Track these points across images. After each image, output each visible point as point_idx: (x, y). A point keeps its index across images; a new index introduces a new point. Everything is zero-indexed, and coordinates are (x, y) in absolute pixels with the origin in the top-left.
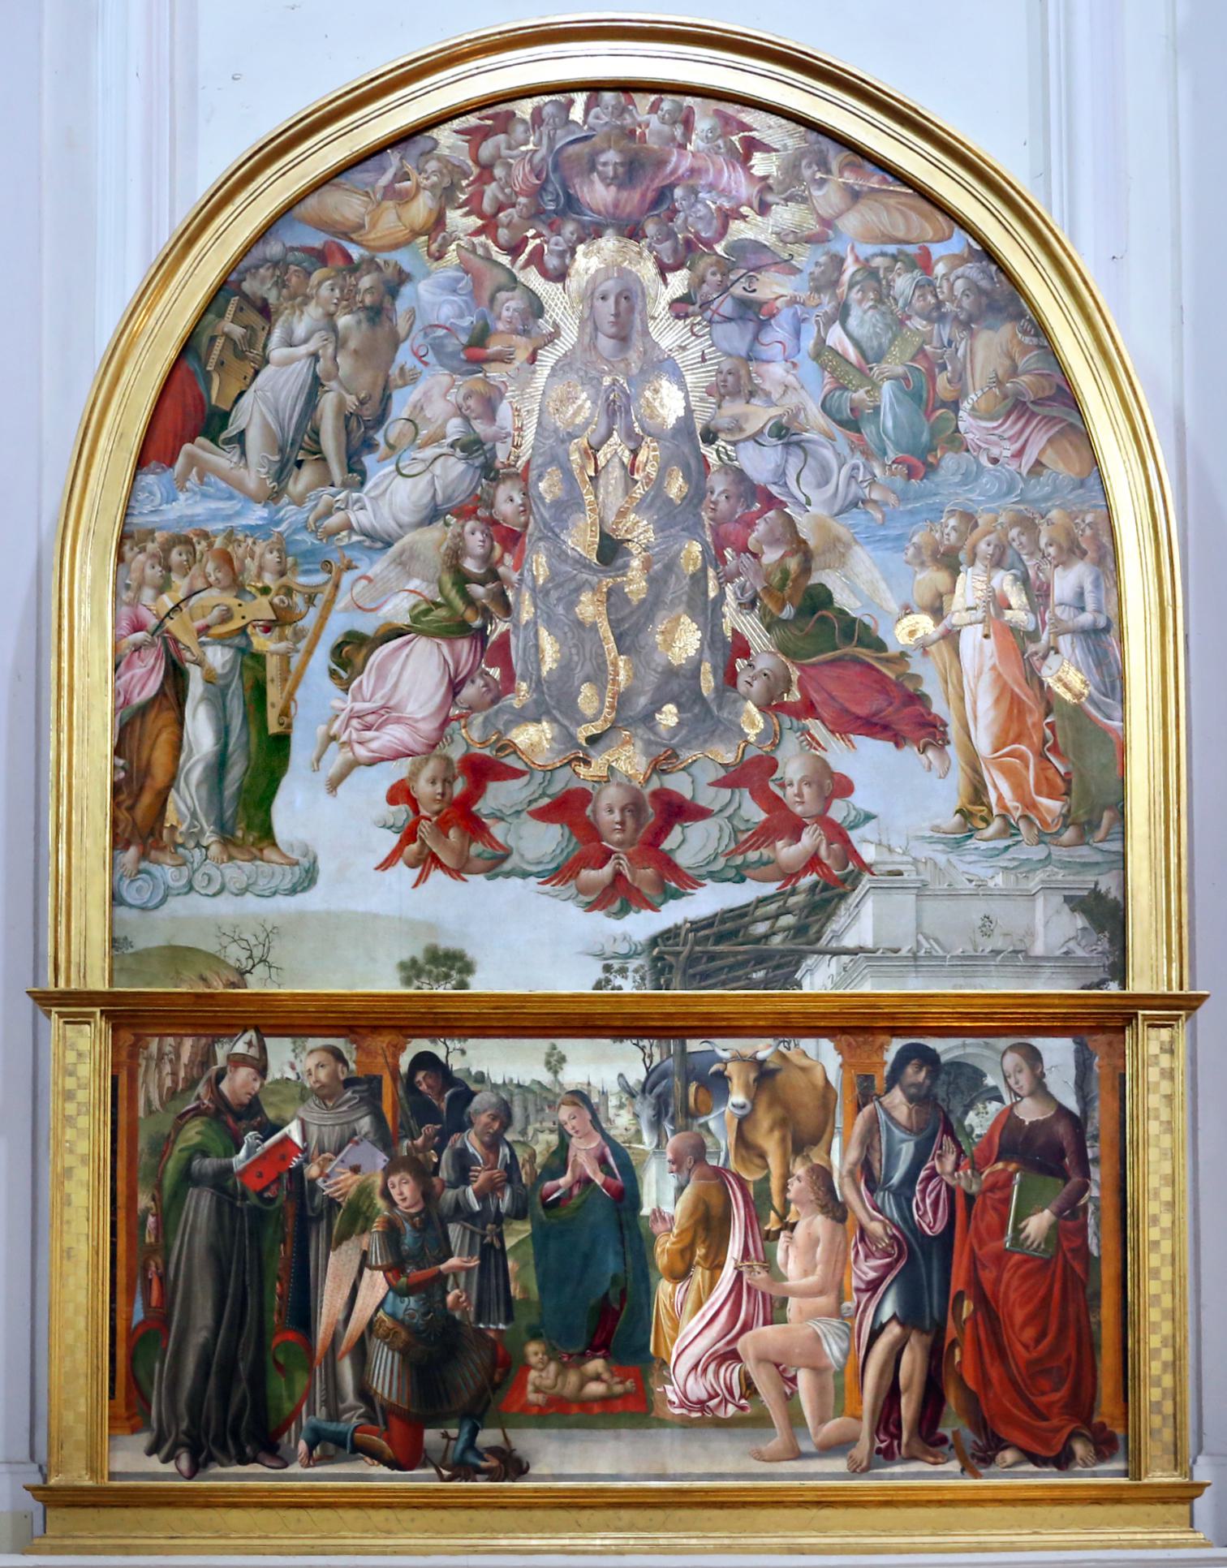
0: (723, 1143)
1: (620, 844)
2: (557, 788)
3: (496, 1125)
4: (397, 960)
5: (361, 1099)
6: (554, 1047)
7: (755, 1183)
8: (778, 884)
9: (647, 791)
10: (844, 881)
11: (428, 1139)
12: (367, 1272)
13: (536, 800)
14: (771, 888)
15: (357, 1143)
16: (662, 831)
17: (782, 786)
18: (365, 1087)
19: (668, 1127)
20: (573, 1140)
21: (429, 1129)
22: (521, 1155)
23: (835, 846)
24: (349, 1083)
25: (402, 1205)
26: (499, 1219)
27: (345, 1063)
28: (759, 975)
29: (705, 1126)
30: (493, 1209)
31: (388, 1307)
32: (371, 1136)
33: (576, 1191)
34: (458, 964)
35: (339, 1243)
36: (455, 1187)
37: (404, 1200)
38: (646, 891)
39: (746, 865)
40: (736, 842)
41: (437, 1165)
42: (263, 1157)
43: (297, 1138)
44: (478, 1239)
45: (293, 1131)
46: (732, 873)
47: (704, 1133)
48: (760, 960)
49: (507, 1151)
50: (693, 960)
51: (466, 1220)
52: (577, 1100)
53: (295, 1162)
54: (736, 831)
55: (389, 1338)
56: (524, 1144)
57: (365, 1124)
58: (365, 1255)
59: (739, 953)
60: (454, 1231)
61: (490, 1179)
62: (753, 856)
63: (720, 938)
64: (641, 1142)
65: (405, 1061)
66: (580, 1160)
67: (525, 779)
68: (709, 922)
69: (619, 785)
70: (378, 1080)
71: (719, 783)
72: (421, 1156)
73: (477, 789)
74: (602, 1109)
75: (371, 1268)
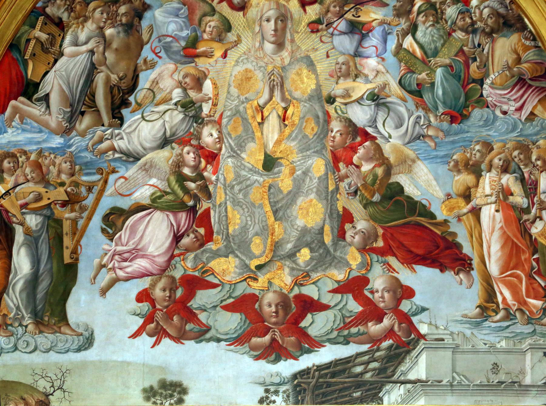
1: (275, 324)
2: (238, 292)
4: (142, 388)
8: (369, 345)
9: (291, 295)
10: (409, 343)
13: (225, 300)
14: (365, 348)
16: (302, 317)
17: (372, 292)
23: (403, 325)
28: (357, 395)
34: (178, 389)
38: (290, 349)
39: (350, 335)
40: (344, 322)
46: (342, 339)
48: (358, 385)
50: (317, 387)
54: (344, 317)
59: (346, 382)
62: (354, 330)
63: (334, 375)
67: (220, 288)
68: (328, 366)
69: (275, 292)
71: (334, 291)
73: (190, 295)
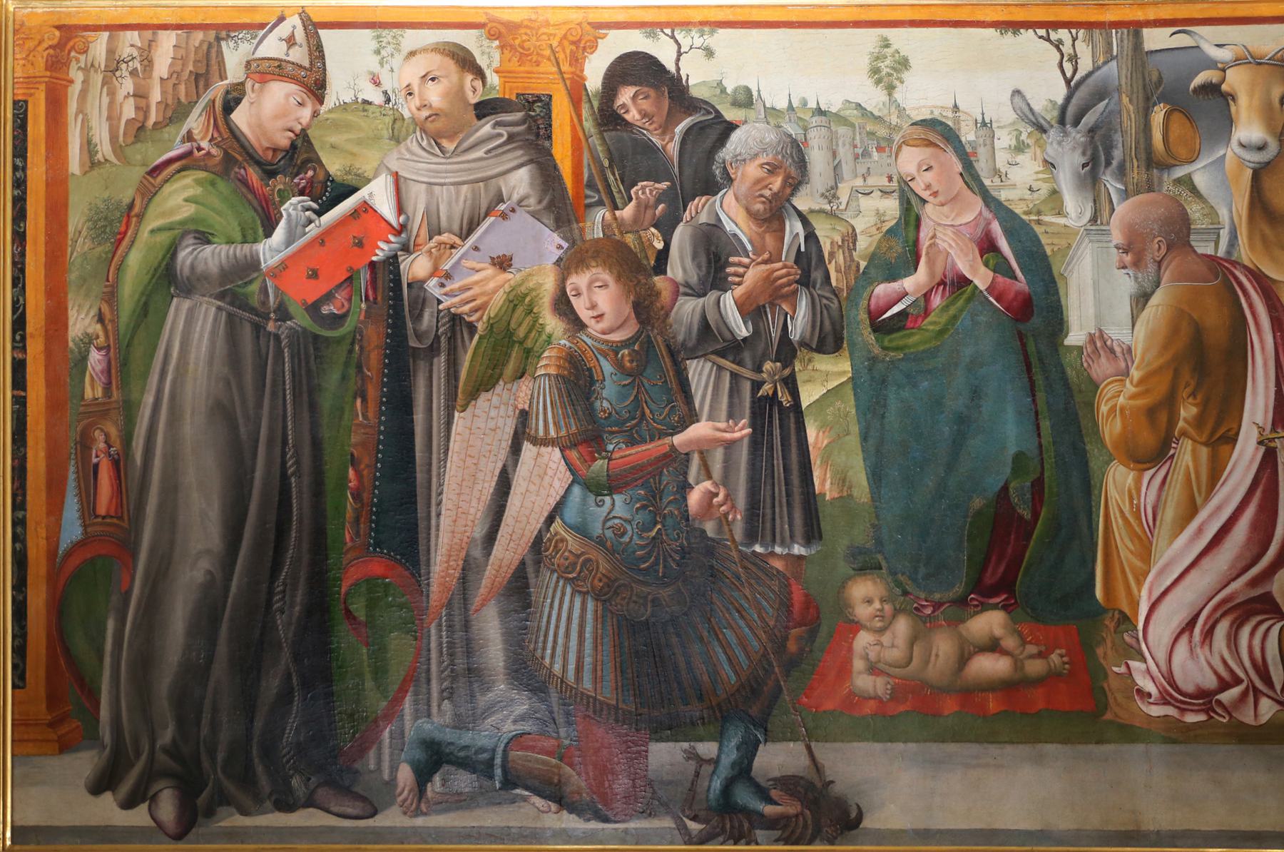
0: (1223, 213)
3: (777, 183)
5: (511, 138)
11: (643, 207)
12: (528, 450)
15: (504, 216)
18: (518, 116)
19: (1112, 184)
20: (929, 208)
21: (645, 190)
22: (827, 235)
24: (484, 109)
25: (594, 328)
26: (786, 351)
27: (479, 73)
29: (1187, 183)
30: (775, 334)
31: (571, 513)
32: (532, 201)
33: (937, 301)
35: (473, 395)
36: (698, 292)
37: (599, 317)
41: (663, 255)
42: (321, 240)
43: (386, 208)
44: (747, 387)
45: (379, 194)
47: (1185, 194)
49: (799, 228)
51: (721, 353)
53: (382, 251)
55: (575, 575)
56: (832, 215)
57: (520, 182)
58: (524, 417)
60: (699, 373)
61: (769, 280)
64: (1060, 212)
65: (594, 73)
66: (942, 245)
70: (546, 102)
72: (630, 239)
74: (982, 152)
75: (536, 441)
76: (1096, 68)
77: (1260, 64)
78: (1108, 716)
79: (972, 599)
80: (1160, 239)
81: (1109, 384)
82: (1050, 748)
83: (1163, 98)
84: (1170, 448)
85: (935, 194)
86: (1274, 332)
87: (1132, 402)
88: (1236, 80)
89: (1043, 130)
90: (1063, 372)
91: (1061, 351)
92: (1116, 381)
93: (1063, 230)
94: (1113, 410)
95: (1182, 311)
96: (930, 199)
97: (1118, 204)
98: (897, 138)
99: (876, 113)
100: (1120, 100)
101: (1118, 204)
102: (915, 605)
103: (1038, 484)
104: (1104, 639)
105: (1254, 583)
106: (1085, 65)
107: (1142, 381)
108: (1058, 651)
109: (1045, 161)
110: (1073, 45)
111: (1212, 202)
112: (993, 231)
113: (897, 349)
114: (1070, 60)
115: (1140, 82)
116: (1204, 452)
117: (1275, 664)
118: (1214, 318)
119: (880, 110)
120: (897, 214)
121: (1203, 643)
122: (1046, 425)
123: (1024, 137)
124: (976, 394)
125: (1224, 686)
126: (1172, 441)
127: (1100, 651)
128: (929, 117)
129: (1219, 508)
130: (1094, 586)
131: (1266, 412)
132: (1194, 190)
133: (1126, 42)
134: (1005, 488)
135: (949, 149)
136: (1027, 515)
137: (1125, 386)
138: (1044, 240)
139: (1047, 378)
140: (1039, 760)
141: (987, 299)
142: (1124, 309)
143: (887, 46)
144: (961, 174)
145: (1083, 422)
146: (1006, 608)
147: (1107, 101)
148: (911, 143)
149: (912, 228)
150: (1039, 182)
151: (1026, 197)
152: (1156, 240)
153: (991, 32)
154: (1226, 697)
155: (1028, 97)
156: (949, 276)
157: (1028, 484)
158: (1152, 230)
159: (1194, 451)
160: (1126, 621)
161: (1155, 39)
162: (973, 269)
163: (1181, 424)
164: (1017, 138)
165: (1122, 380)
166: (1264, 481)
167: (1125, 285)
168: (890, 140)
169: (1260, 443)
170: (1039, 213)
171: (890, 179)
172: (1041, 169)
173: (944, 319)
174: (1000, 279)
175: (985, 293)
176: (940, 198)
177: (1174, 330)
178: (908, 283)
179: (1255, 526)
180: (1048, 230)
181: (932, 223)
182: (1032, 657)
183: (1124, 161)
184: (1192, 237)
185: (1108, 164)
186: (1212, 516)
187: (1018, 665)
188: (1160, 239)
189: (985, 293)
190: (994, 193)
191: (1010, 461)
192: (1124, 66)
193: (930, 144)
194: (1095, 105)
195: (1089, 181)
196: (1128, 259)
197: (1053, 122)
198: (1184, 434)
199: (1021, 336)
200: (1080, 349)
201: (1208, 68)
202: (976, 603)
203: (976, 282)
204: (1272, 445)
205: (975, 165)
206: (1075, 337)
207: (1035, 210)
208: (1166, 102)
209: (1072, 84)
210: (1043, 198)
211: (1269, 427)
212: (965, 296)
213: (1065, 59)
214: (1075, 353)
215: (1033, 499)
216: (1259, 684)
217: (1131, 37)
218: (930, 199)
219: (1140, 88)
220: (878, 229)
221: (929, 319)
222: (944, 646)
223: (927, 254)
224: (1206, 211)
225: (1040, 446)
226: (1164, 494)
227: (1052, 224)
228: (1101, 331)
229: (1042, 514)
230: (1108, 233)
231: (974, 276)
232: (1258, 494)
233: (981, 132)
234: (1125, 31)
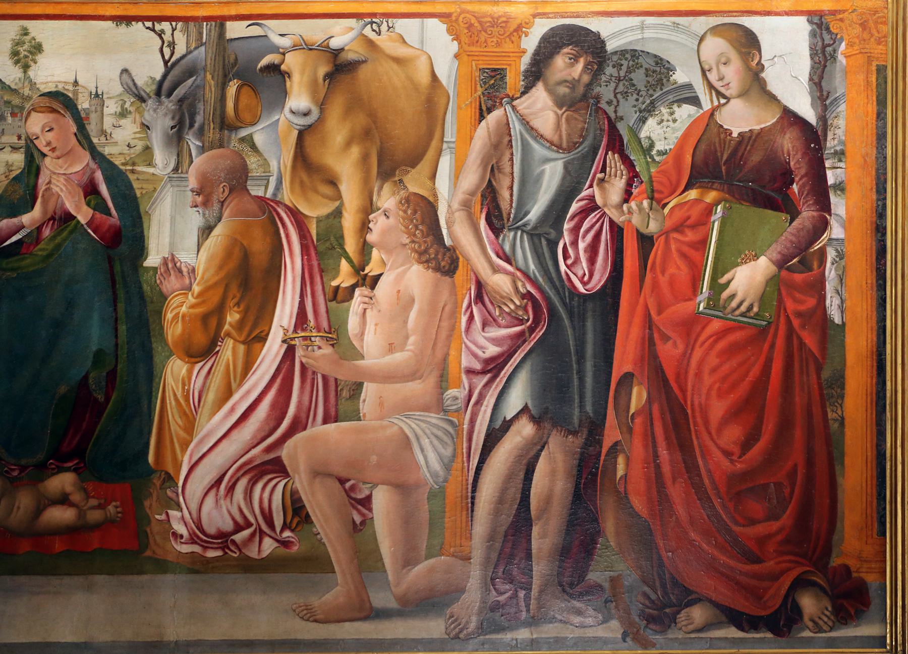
0: (274, 165)
6: (25, 32)
7: (319, 220)
19: (192, 142)
20: (47, 161)
29: (249, 141)
33: (47, 232)
47: (247, 149)
52: (57, 106)
64: (150, 164)
66: (55, 189)
74: (93, 117)
76: (189, 52)
77: (311, 49)
78: (148, 553)
79: (51, 463)
80: (225, 184)
81: (171, 300)
82: (100, 579)
83: (237, 76)
84: (216, 345)
85: (53, 150)
86: (302, 256)
87: (191, 311)
88: (292, 62)
89: (142, 100)
90: (141, 288)
91: (141, 271)
92: (181, 294)
93: (152, 178)
94: (176, 316)
95: (236, 240)
96: (50, 153)
97: (197, 157)
98: (28, 106)
99: (13, 86)
100: (205, 77)
101: (197, 157)
102: (6, 469)
103: (112, 375)
104: (151, 494)
105: (269, 449)
106: (180, 49)
107: (200, 294)
108: (114, 503)
109: (143, 124)
110: (172, 34)
111: (266, 155)
112: (96, 178)
113: (13, 270)
114: (169, 46)
115: (221, 63)
116: (241, 348)
117: (278, 512)
118: (259, 246)
119: (16, 84)
120: (22, 165)
121: (226, 496)
122: (122, 328)
123: (127, 105)
124: (70, 305)
125: (238, 528)
126: (218, 340)
127: (147, 503)
128: (54, 89)
129: (248, 392)
130: (147, 453)
131: (291, 317)
132: (254, 147)
133: (213, 32)
134: (86, 377)
135: (68, 115)
136: (101, 397)
137: (187, 298)
138: (136, 185)
139: (127, 292)
140: (89, 588)
141: (86, 231)
142: (192, 238)
143: (26, 34)
144: (75, 134)
145: (152, 327)
146: (76, 470)
147: (194, 78)
148: (38, 109)
149: (33, 177)
150: (136, 141)
151: (125, 152)
152: (222, 186)
153: (109, 24)
154: (239, 537)
155: (133, 74)
156: (58, 212)
157: (105, 374)
158: (219, 177)
159: (234, 349)
160: (170, 479)
161: (235, 30)
162: (78, 208)
163: (227, 327)
164: (122, 107)
165: (184, 294)
166: (283, 371)
167: (195, 219)
168: (22, 108)
169: (284, 341)
170: (134, 164)
171: (19, 138)
172: (139, 130)
173: (51, 246)
174: (98, 215)
175: (85, 226)
176: (57, 153)
177: (228, 254)
178: (26, 219)
179: (274, 406)
180: (140, 177)
181: (49, 172)
182: (93, 508)
183: (204, 124)
184: (249, 182)
185: (191, 126)
186: (243, 398)
187: (81, 514)
188: (225, 184)
189: (85, 226)
190: (100, 149)
191: (91, 356)
192: (210, 51)
193: (53, 111)
194: (185, 81)
195: (175, 139)
196: (199, 199)
197: (152, 94)
198: (228, 335)
199: (110, 260)
200: (155, 269)
201: (272, 52)
202: (54, 466)
203: (80, 218)
204: (293, 343)
205: (87, 126)
206: (152, 260)
207: (130, 162)
208: (239, 79)
209: (169, 64)
210: (138, 152)
211: (292, 328)
212: (69, 229)
213: (166, 45)
214: (151, 272)
215: (107, 386)
216: (264, 527)
217: (217, 29)
218: (50, 153)
219: (221, 67)
220: (6, 177)
221: (39, 247)
222: (24, 501)
223: (43, 196)
224: (261, 162)
225: (117, 345)
226: (209, 381)
227: (143, 173)
228: (173, 255)
229: (113, 398)
230: (186, 179)
231: (78, 213)
232: (279, 381)
233: (94, 102)
234: (214, 23)
